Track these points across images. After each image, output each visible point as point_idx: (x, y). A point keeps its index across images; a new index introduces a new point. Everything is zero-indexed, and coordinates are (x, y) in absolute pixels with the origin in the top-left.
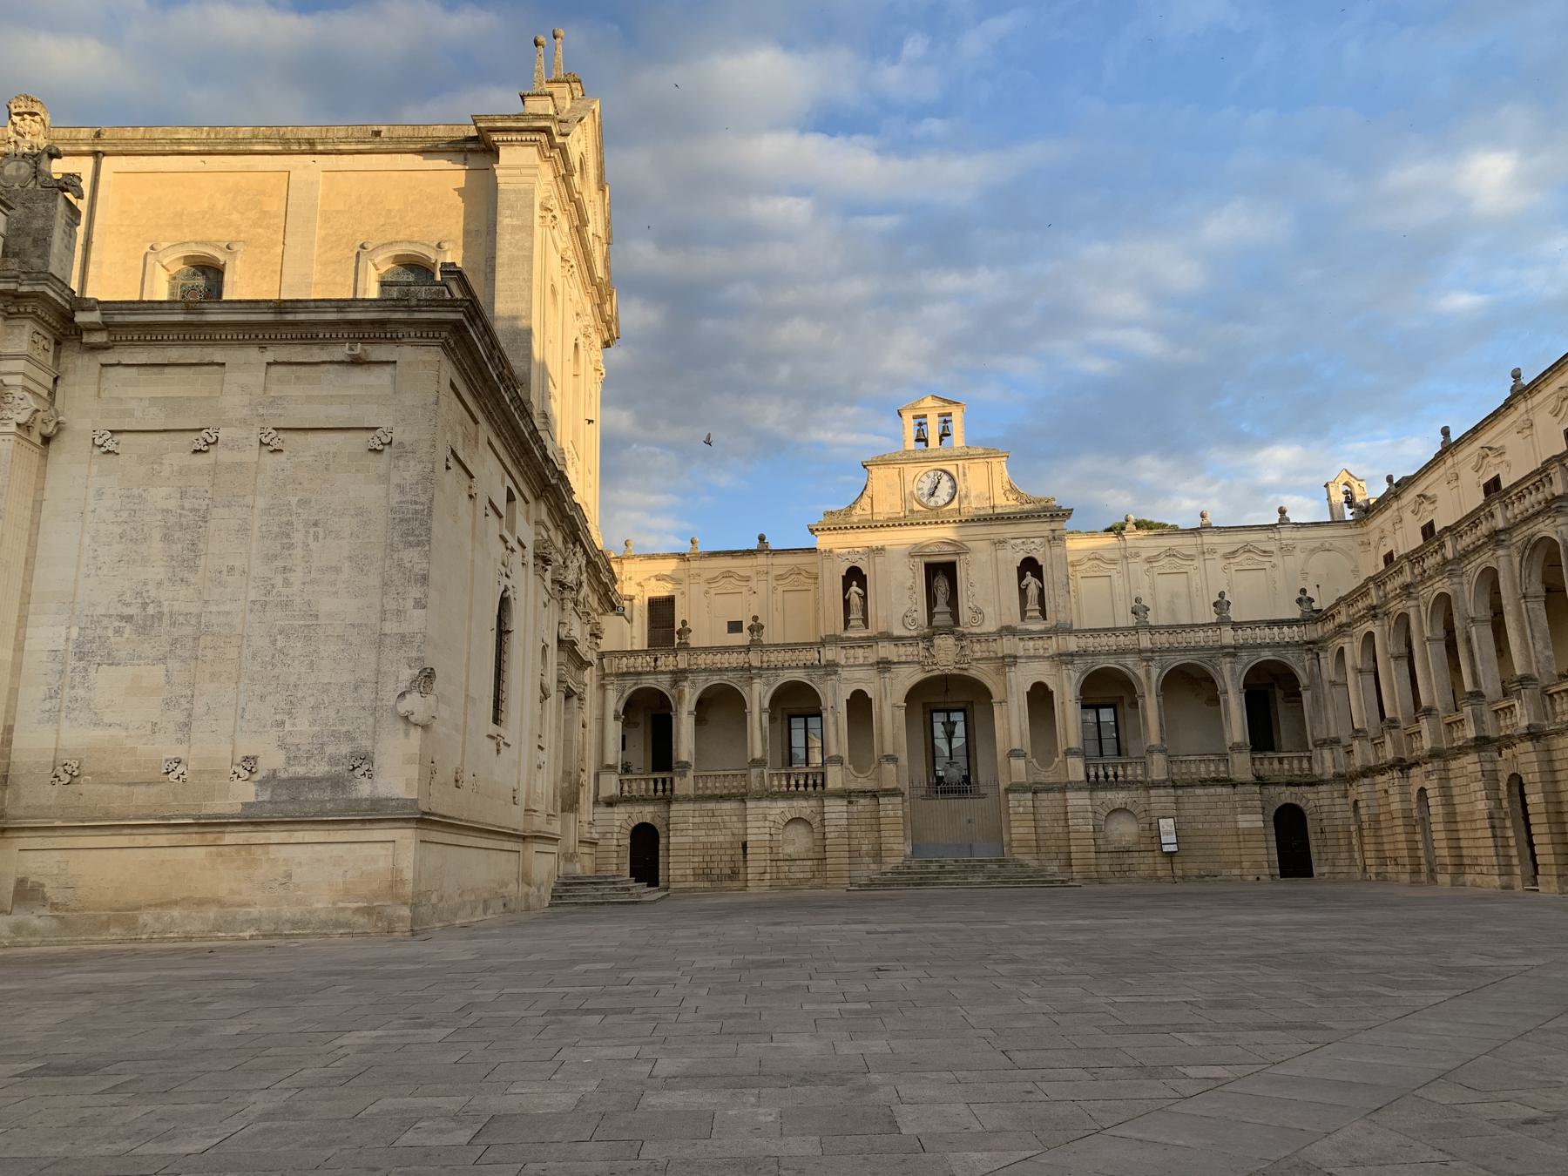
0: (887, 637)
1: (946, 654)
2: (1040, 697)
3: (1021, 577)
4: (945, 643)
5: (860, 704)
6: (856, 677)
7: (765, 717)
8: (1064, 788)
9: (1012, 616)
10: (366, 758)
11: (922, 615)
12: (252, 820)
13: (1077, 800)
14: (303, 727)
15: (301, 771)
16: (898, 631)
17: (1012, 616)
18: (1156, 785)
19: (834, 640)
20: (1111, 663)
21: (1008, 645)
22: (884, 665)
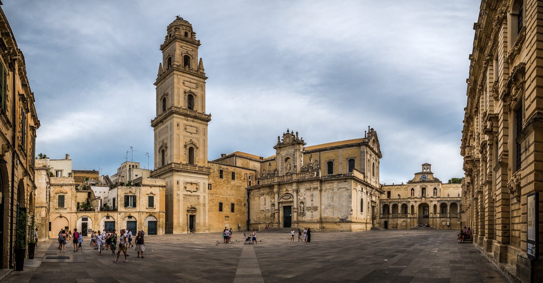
0: (416, 198)
1: (423, 200)
2: (435, 206)
3: (434, 190)
4: (423, 199)
5: (413, 207)
6: (412, 203)
7: (401, 208)
8: (436, 218)
9: (432, 195)
10: (347, 217)
11: (421, 195)
12: (339, 222)
13: (438, 219)
14: (342, 214)
15: (342, 218)
16: (418, 197)
17: (432, 195)
18: (448, 218)
19: (409, 198)
20: (444, 202)
21: (431, 199)
22: (416, 202)
